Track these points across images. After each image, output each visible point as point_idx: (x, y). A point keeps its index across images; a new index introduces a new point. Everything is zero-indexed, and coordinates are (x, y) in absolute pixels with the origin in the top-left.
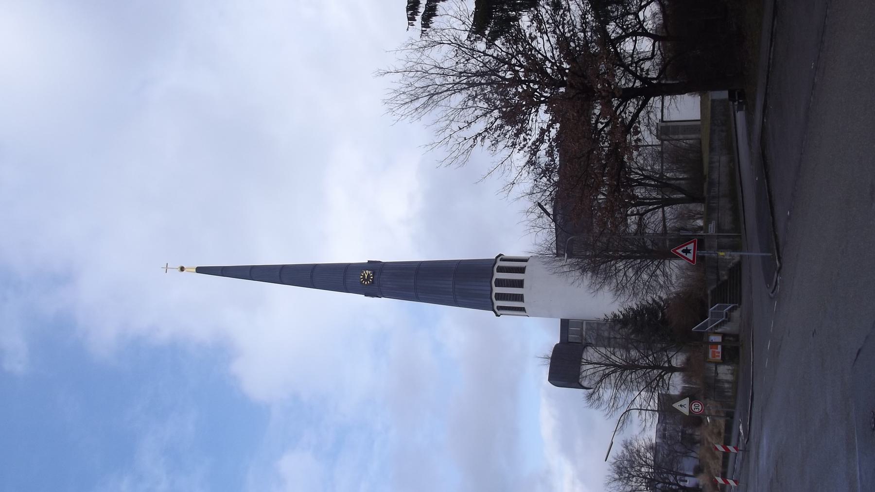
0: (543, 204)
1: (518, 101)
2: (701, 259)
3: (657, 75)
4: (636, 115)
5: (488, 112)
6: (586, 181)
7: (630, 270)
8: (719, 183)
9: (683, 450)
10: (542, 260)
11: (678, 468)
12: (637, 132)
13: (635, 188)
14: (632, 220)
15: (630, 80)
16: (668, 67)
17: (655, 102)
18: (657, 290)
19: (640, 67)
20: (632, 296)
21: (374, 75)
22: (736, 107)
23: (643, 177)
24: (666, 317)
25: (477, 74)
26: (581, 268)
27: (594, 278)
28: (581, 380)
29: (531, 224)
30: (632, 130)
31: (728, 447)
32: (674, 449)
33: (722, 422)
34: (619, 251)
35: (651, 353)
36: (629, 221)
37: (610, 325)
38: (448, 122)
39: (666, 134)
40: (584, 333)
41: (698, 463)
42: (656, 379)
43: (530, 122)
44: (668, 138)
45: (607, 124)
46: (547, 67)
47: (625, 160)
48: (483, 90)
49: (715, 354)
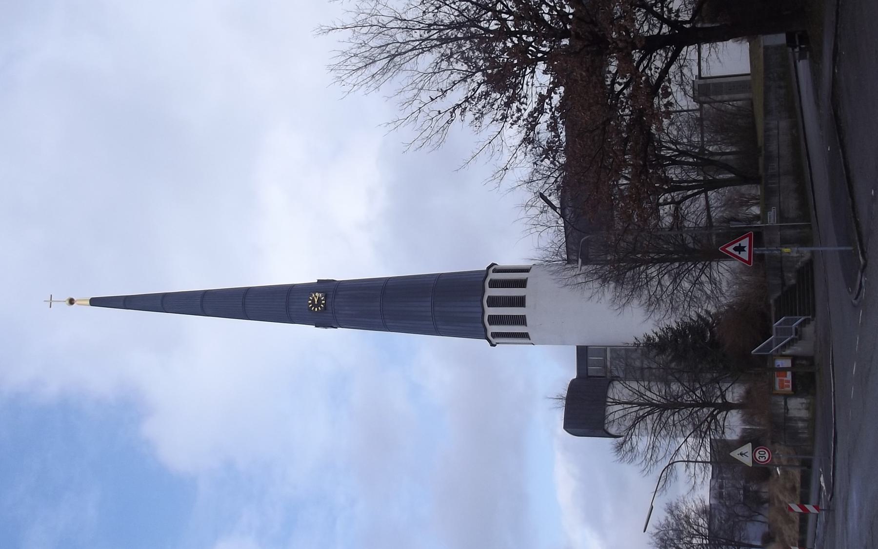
0: (546, 194)
1: (508, 59)
2: (760, 258)
3: (690, 16)
4: (665, 72)
5: (468, 76)
6: (602, 162)
7: (666, 277)
8: (779, 158)
9: (747, 513)
10: (548, 270)
11: (740, 538)
12: (667, 94)
13: (668, 168)
14: (666, 211)
15: (654, 25)
16: (705, 6)
17: (689, 52)
18: (703, 303)
19: (667, 7)
20: (670, 311)
21: (314, 33)
22: (797, 55)
23: (677, 153)
24: (716, 337)
25: (451, 26)
26: (600, 277)
27: (619, 290)
28: (606, 425)
29: (532, 222)
30: (660, 91)
31: (806, 506)
32: (734, 511)
33: (796, 473)
34: (650, 253)
35: (698, 386)
36: (661, 212)
37: (642, 352)
38: (416, 91)
39: (706, 95)
40: (608, 364)
41: (767, 529)
42: (706, 420)
43: (525, 86)
44: (709, 99)
45: (627, 85)
46: (544, 13)
47: (652, 132)
48: (460, 46)
49: (783, 384)
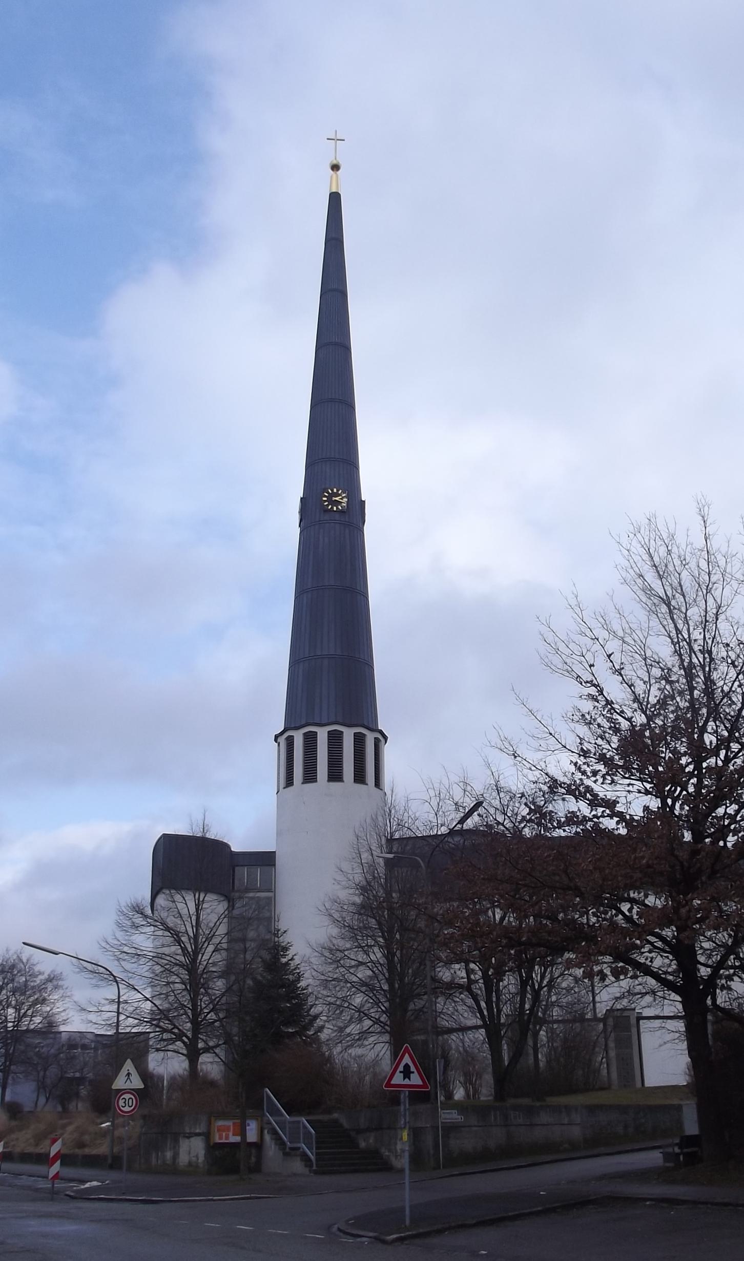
0: (481, 810)
1: (664, 758)
2: (394, 1100)
3: (722, 1005)
4: (647, 971)
5: (641, 704)
6: (525, 885)
7: (369, 973)
9: (48, 1081)
10: (379, 813)
11: (16, 1073)
12: (617, 974)
13: (517, 975)
14: (459, 972)
16: (736, 1025)
17: (673, 1004)
18: (334, 1022)
19: (734, 974)
20: (323, 977)
21: (700, 497)
22: (670, 1150)
23: (537, 987)
24: (287, 1041)
25: (709, 681)
26: (368, 883)
27: (351, 909)
28: (168, 892)
29: (444, 791)
30: (621, 964)
31: (59, 1162)
32: (51, 1065)
33: (103, 1149)
34: (401, 951)
35: (221, 1015)
36: (457, 966)
37: (267, 940)
38: (620, 633)
39: (615, 1027)
40: (251, 895)
41: (27, 1109)
42: (175, 1027)
43: (627, 781)
44: (610, 1030)
45: (628, 919)
46: (727, 807)
47: (566, 954)
48: (681, 693)
49: (224, 1131)
